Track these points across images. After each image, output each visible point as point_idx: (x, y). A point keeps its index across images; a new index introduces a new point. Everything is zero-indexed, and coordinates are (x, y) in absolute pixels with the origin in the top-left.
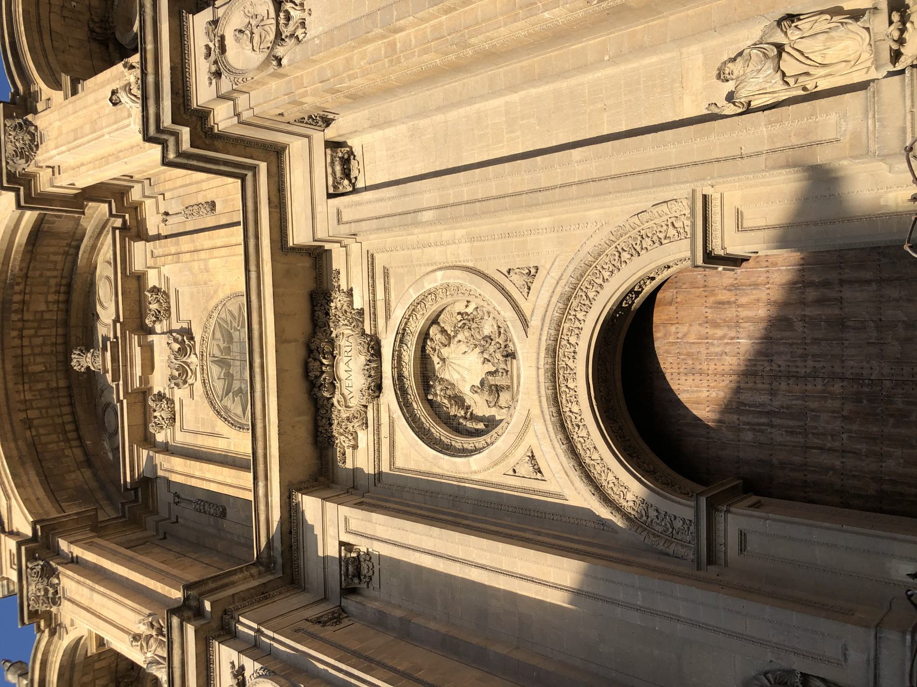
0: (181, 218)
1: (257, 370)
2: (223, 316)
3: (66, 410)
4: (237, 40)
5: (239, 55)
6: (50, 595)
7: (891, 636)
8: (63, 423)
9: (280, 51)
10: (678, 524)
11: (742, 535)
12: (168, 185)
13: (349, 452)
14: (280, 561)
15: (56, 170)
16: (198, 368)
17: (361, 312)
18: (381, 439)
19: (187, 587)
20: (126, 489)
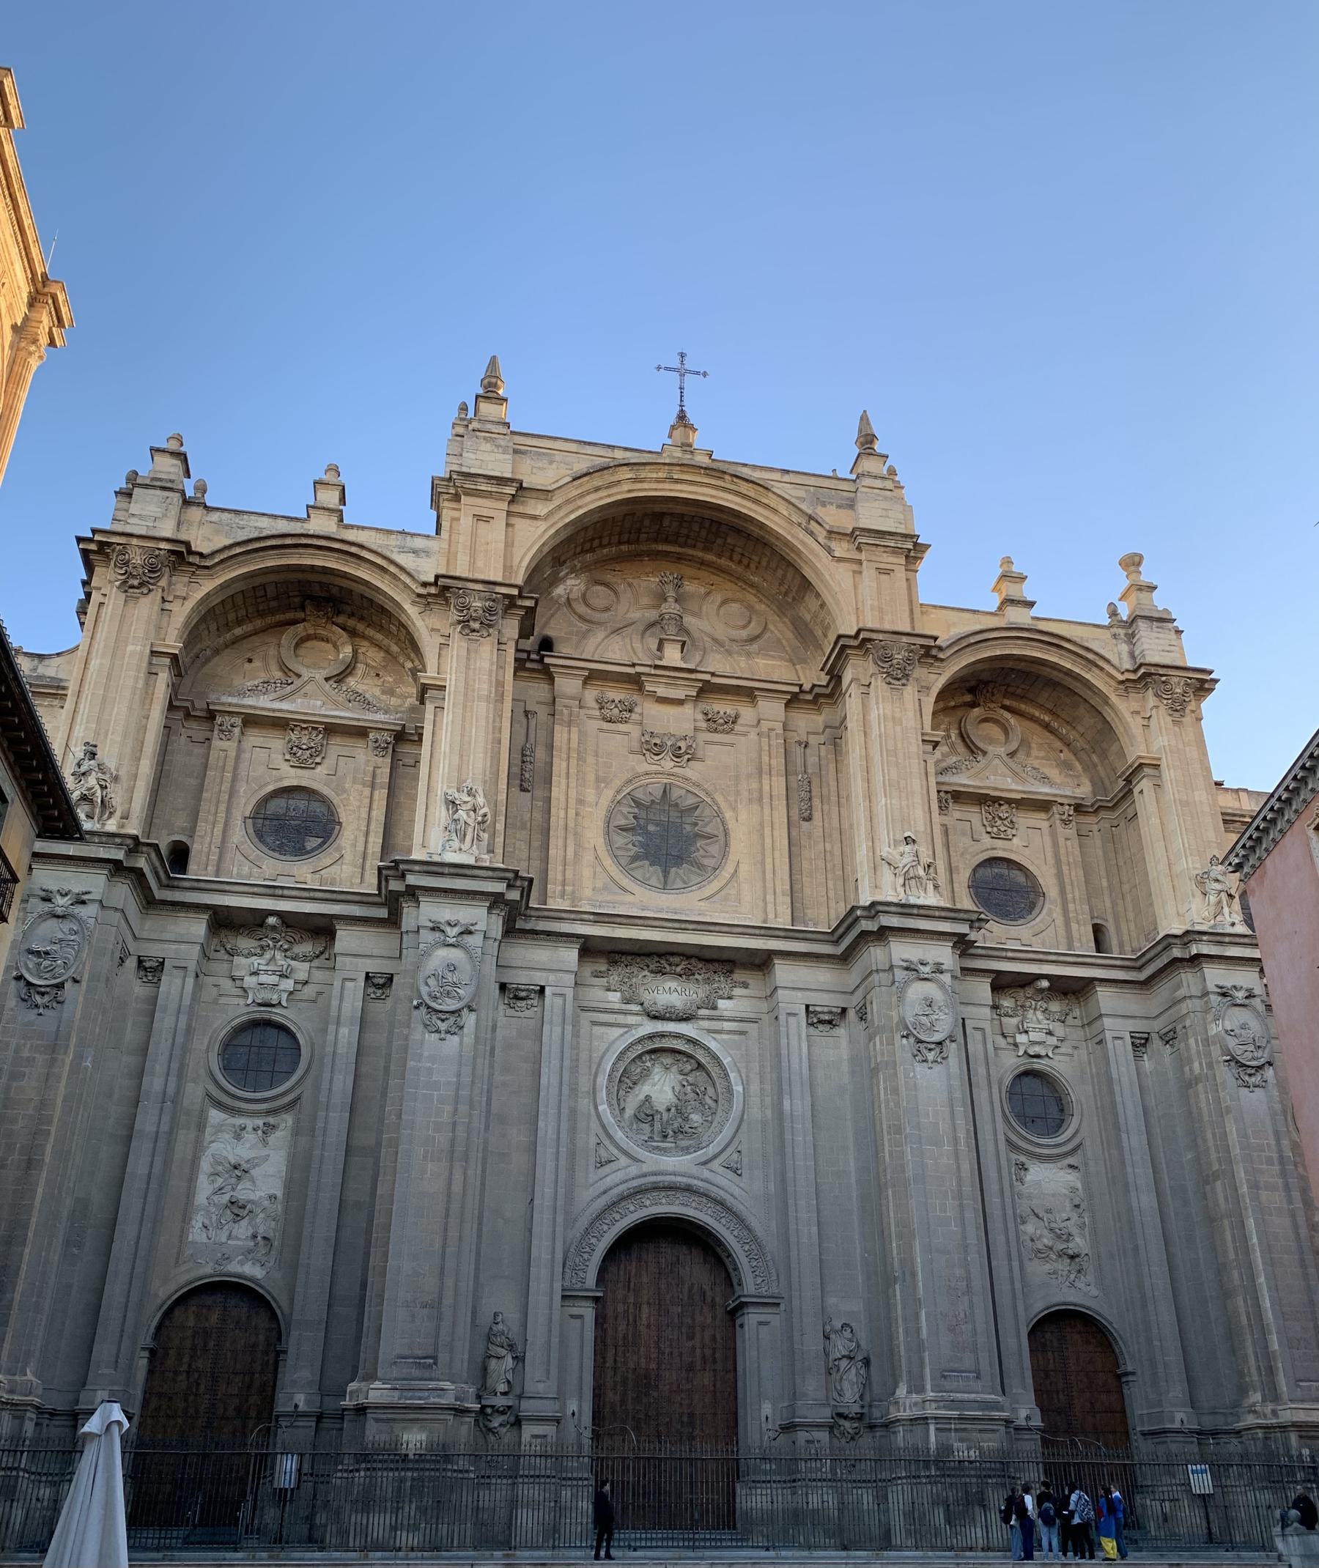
0: (800, 768)
1: (683, 926)
2: (707, 812)
3: (615, 539)
4: (926, 999)
5: (917, 991)
6: (471, 623)
7: (557, 1407)
8: (601, 538)
9: (912, 1040)
10: (581, 1274)
11: (581, 1317)
12: (832, 766)
13: (603, 981)
14: (528, 926)
15: (864, 690)
16: (659, 768)
17: (715, 1008)
18: (616, 1018)
19: (531, 881)
20: (543, 656)
